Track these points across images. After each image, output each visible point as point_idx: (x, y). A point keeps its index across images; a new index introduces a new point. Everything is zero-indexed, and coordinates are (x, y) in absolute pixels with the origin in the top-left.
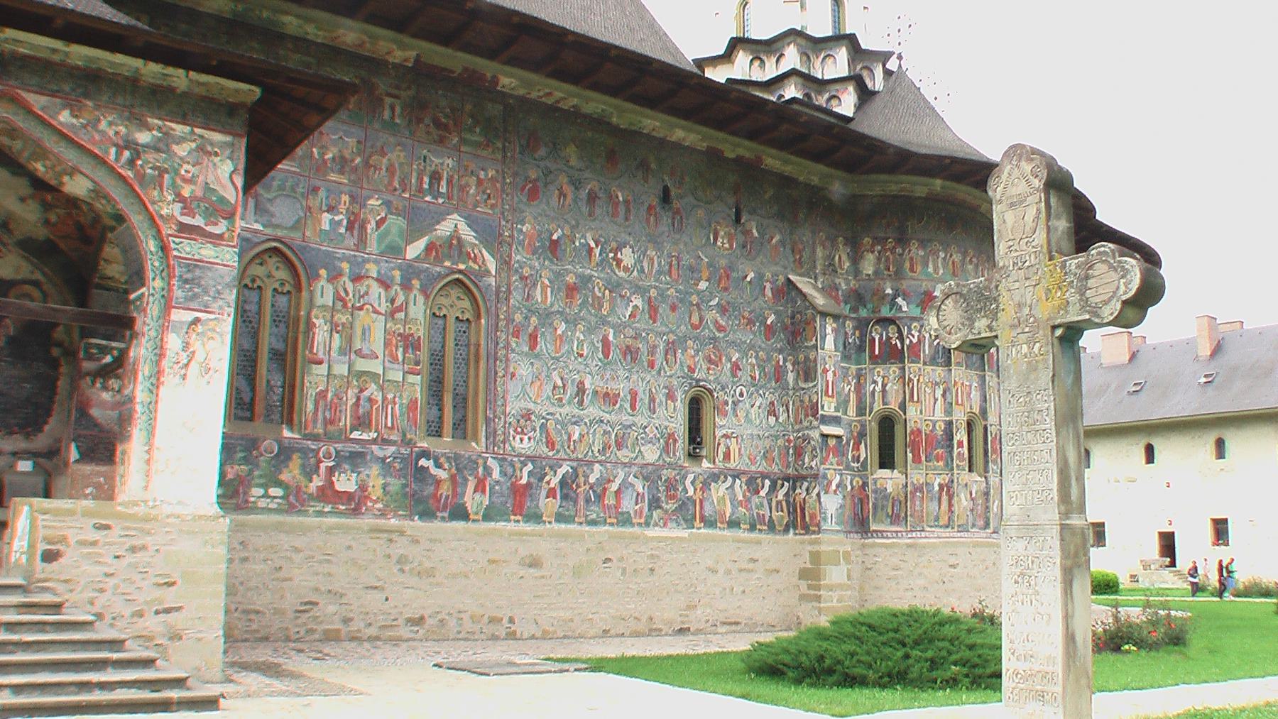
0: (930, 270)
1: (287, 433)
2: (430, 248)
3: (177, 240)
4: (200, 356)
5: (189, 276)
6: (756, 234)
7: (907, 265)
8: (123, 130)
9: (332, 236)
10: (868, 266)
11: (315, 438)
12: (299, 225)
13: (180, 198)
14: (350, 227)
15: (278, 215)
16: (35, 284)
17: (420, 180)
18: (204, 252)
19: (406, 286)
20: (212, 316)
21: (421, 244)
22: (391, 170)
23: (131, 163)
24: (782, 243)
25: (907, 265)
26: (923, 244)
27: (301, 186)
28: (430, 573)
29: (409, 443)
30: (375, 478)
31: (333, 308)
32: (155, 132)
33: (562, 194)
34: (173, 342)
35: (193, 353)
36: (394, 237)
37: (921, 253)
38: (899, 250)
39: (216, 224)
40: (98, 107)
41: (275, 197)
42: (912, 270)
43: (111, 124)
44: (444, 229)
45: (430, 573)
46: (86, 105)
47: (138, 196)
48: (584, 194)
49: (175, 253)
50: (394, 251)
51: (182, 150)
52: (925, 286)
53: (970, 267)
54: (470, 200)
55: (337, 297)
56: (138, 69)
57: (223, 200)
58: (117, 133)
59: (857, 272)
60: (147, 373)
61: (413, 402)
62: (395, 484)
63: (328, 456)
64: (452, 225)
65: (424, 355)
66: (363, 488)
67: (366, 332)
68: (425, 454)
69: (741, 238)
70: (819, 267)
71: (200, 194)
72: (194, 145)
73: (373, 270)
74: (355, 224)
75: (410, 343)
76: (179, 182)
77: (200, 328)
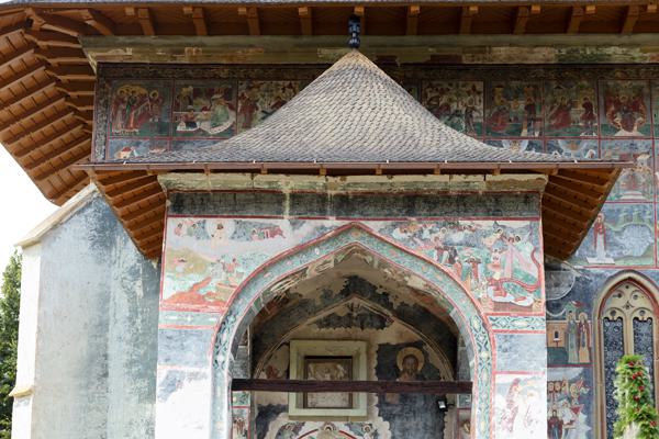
3: (494, 317)
4: (522, 411)
5: (506, 345)
8: (440, 235)
13: (492, 282)
15: (627, 245)
16: (417, 345)
18: (516, 323)
20: (530, 377)
23: (451, 260)
27: (648, 212)
32: (466, 231)
34: (499, 401)
35: (517, 408)
39: (525, 298)
40: (419, 220)
41: (624, 229)
43: (431, 232)
46: (410, 222)
47: (462, 289)
49: (494, 328)
56: (446, 183)
57: (527, 276)
58: (437, 238)
60: (482, 428)
71: (508, 276)
72: (498, 235)
76: (489, 267)
77: (520, 388)
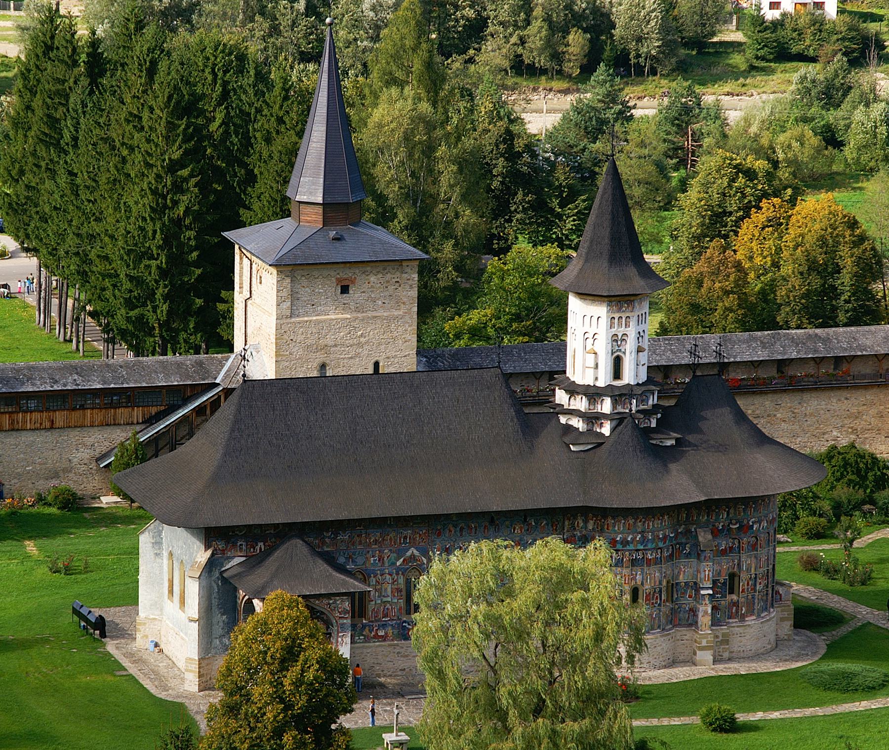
0: (616, 529)
1: (364, 621)
2: (403, 561)
6: (533, 524)
7: (606, 527)
9: (374, 564)
10: (590, 526)
11: (372, 622)
12: (364, 563)
14: (379, 560)
17: (400, 540)
19: (397, 574)
21: (402, 560)
22: (391, 539)
24: (547, 524)
25: (606, 527)
26: (613, 518)
28: (407, 656)
29: (399, 619)
30: (390, 631)
31: (376, 585)
33: (450, 531)
34: (340, 639)
36: (393, 560)
37: (613, 521)
38: (603, 520)
42: (608, 529)
44: (409, 554)
45: (407, 656)
48: (458, 529)
50: (394, 564)
51: (338, 602)
52: (612, 536)
53: (639, 524)
54: (417, 543)
55: (377, 581)
59: (586, 528)
61: (401, 608)
62: (396, 631)
63: (376, 626)
64: (413, 551)
65: (404, 593)
66: (386, 633)
67: (386, 589)
68: (405, 622)
69: (526, 527)
70: (566, 529)
73: (387, 571)
74: (381, 559)
75: (399, 590)
